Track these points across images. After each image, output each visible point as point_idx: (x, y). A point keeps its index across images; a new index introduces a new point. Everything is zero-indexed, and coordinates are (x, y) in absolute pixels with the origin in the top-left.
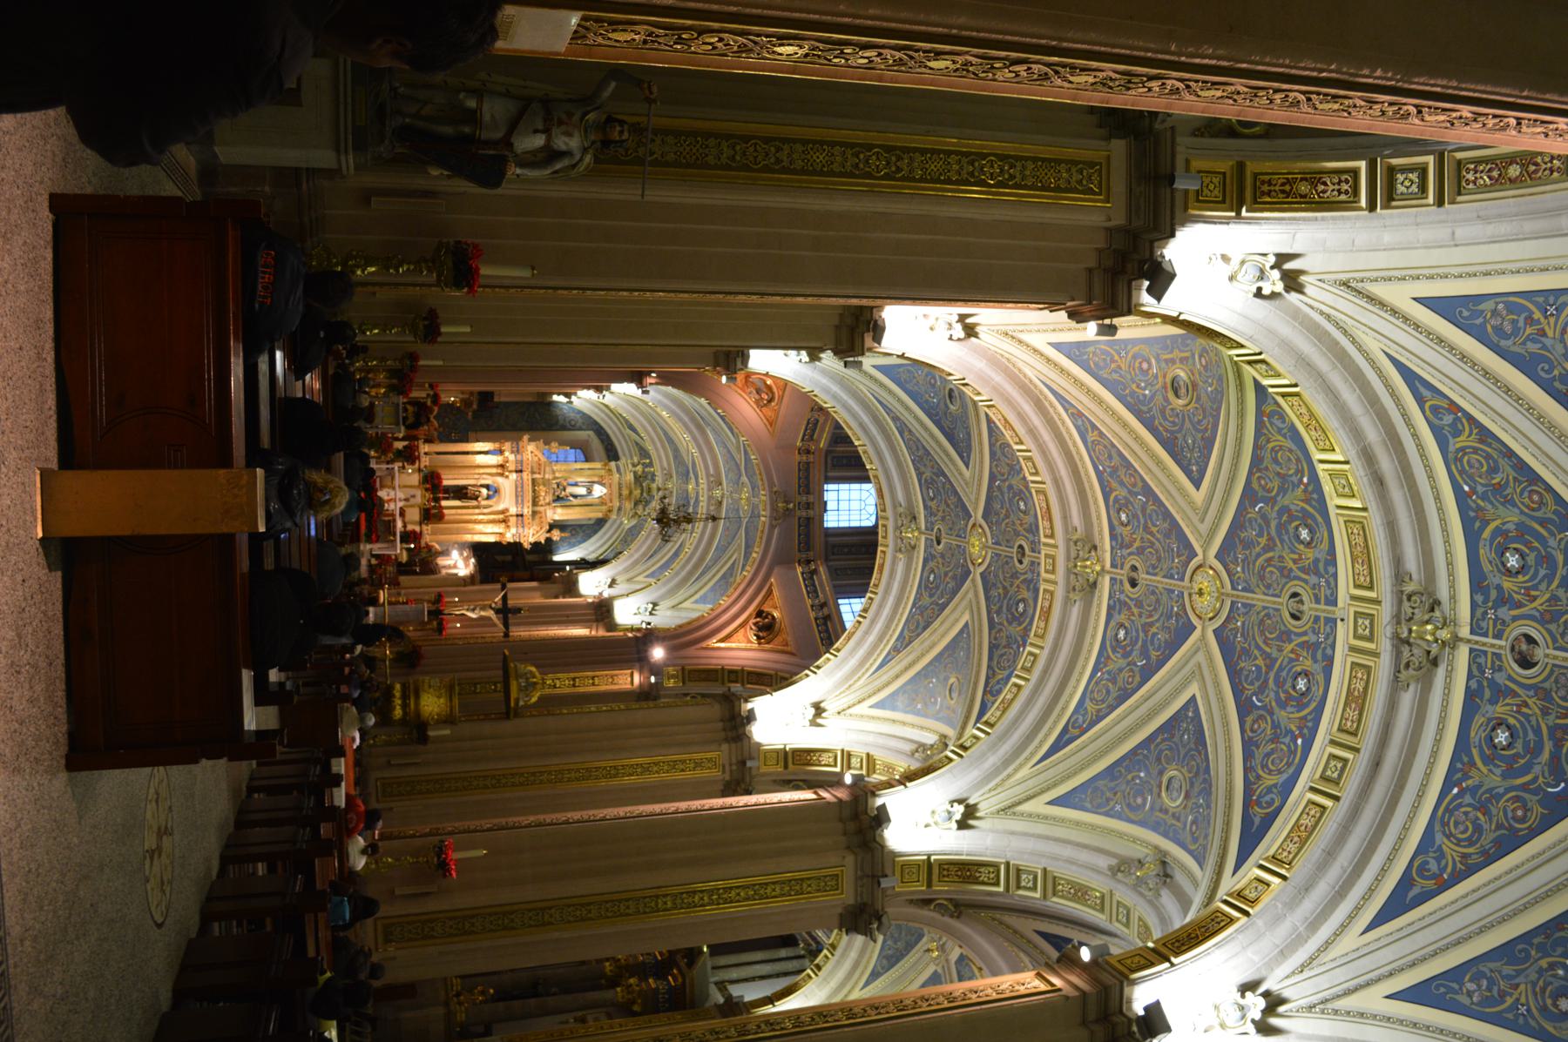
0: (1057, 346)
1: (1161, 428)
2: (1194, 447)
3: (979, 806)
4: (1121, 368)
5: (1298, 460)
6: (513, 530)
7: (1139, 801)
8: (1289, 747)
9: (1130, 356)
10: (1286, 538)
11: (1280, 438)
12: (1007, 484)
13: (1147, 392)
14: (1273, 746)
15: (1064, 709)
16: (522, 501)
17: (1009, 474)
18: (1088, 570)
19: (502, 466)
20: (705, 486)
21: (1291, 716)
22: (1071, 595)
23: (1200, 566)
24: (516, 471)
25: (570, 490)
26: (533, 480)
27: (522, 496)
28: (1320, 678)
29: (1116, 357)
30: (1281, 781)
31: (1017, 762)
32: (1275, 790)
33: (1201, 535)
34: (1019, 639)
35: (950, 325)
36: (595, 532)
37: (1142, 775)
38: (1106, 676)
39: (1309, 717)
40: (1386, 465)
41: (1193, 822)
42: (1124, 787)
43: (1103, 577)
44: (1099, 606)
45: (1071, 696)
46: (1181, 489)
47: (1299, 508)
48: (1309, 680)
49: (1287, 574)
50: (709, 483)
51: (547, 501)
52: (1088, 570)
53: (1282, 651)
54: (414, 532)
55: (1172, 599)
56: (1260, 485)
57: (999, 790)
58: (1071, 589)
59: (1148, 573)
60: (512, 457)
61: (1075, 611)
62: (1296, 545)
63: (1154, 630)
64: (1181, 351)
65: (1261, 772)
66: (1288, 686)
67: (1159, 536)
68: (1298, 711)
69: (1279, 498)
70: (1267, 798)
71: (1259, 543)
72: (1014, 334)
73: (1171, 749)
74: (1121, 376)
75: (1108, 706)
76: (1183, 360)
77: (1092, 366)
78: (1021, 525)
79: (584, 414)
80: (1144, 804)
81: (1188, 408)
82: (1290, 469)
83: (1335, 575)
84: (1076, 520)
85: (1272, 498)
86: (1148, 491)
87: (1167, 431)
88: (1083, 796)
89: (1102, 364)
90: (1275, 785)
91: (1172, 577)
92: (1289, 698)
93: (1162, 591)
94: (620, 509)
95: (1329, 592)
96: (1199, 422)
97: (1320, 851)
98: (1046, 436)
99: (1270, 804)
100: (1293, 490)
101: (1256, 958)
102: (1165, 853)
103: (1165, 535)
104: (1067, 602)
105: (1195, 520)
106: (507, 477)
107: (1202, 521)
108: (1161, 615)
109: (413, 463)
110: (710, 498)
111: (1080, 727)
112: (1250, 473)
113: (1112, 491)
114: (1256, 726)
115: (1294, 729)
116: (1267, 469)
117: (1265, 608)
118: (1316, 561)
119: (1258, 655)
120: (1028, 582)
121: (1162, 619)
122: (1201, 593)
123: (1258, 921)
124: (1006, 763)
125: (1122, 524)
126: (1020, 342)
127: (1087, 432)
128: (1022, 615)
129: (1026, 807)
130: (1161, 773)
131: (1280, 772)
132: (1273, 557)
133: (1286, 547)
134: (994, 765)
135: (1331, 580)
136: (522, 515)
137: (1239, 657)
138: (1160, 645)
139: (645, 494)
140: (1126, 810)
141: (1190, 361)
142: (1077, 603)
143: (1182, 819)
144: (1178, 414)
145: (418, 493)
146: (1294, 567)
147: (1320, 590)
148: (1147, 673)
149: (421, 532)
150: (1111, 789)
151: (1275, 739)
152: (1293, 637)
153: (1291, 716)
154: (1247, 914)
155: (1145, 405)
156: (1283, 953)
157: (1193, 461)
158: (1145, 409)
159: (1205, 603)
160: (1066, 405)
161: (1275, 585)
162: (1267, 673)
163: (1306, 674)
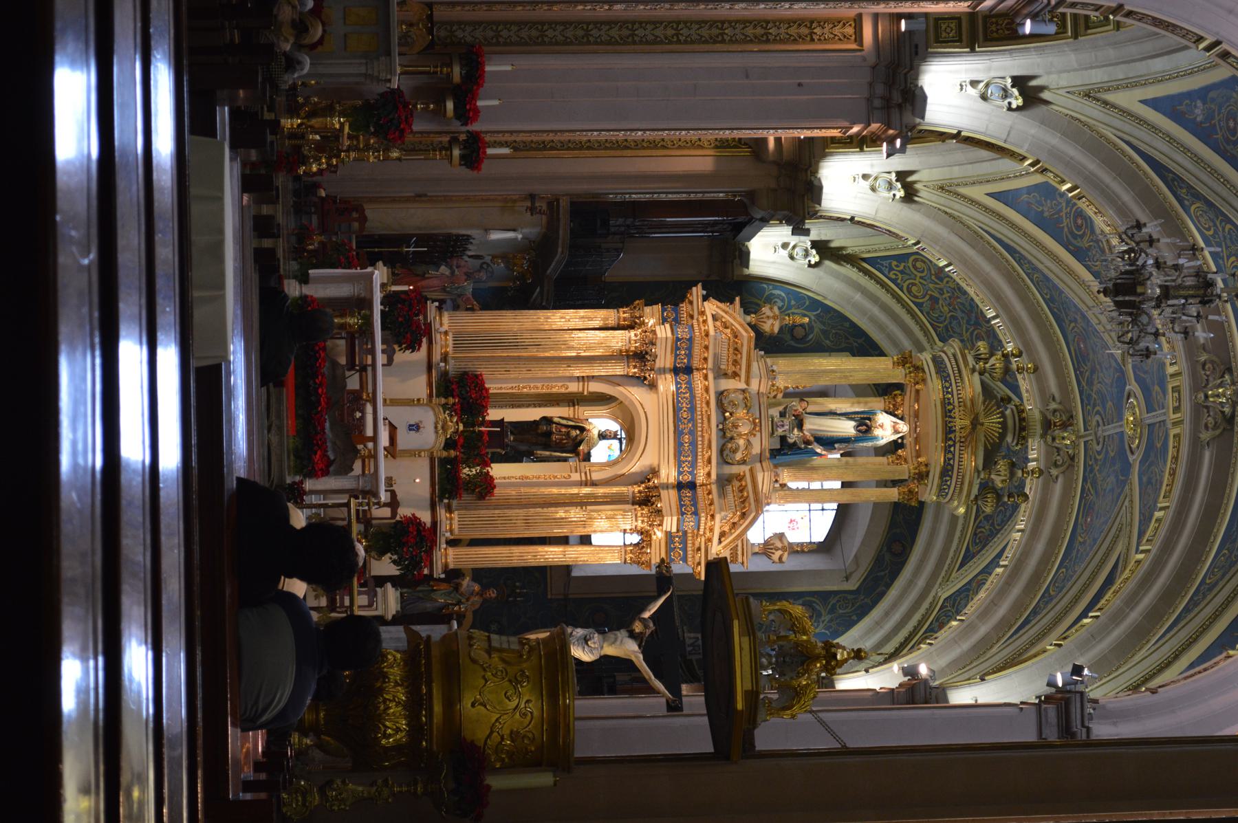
6: (670, 523)
16: (693, 444)
19: (640, 357)
20: (1184, 382)
24: (676, 371)
25: (813, 425)
26: (720, 395)
27: (692, 433)
36: (863, 612)
50: (1195, 367)
51: (756, 450)
54: (414, 521)
60: (664, 332)
79: (828, 309)
94: (946, 472)
106: (653, 386)
109: (413, 346)
110: (1199, 409)
136: (692, 486)
139: (1009, 439)
145: (427, 417)
149: (434, 523)
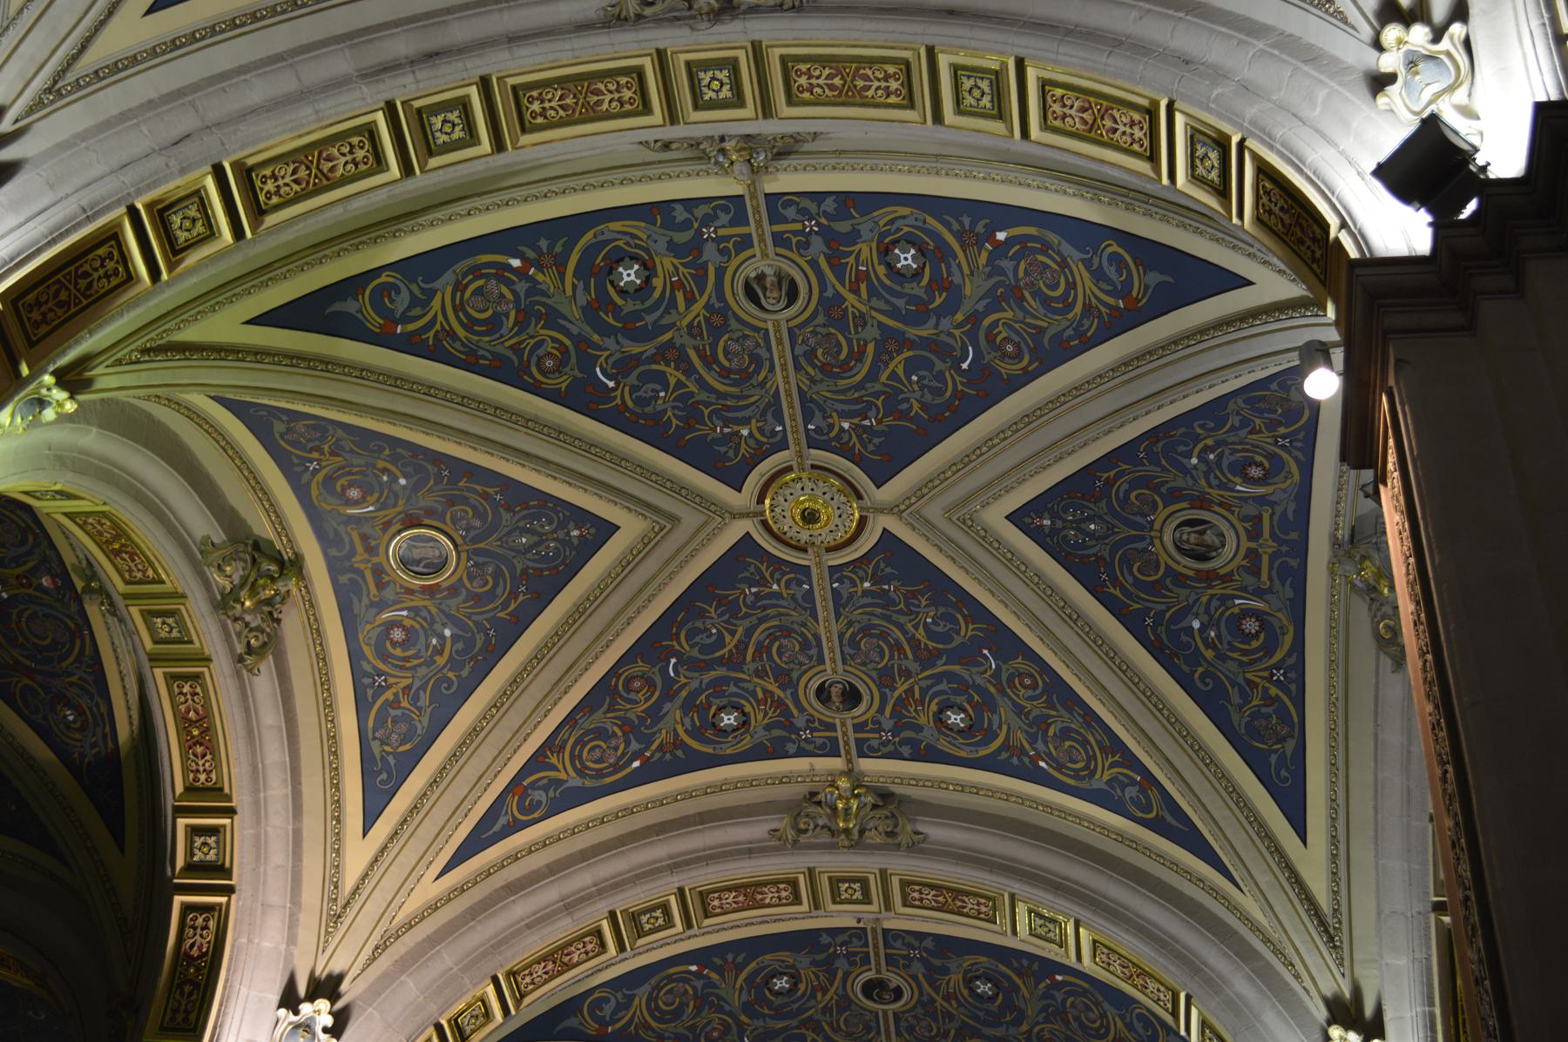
0: (370, 819)
1: (512, 607)
2: (531, 532)
3: (1328, 993)
4: (409, 687)
5: (476, 271)
7: (1251, 626)
8: (1018, 258)
9: (381, 666)
10: (650, 319)
11: (436, 304)
12: (743, 1018)
13: (447, 633)
14: (1027, 294)
15: (1121, 837)
17: (720, 1009)
18: (854, 804)
21: (966, 271)
22: (903, 839)
23: (764, 523)
28: (883, 215)
29: (389, 695)
30: (1077, 255)
31: (1243, 931)
32: (1096, 261)
33: (705, 524)
34: (1042, 985)
35: (297, 1026)
37: (1196, 625)
38: (1040, 746)
39: (956, 226)
40: (400, 46)
41: (1249, 480)
42: (1230, 664)
43: (863, 774)
44: (917, 781)
45: (1104, 828)
46: (627, 564)
47: (581, 286)
48: (895, 242)
49: (719, 319)
52: (854, 804)
53: (862, 315)
55: (852, 595)
56: (557, 370)
57: (1290, 951)
58: (892, 839)
59: (821, 661)
61: (937, 832)
62: (657, 294)
63: (921, 634)
64: (353, 552)
65: (1078, 308)
66: (918, 289)
67: (740, 630)
68: (955, 257)
69: (575, 331)
70: (1111, 272)
71: (679, 384)
72: (341, 902)
73: (1126, 562)
74: (423, 687)
75: (1089, 727)
76: (371, 550)
77: (408, 747)
78: (825, 991)
80: (1257, 615)
81: (459, 541)
82: (502, 296)
83: (689, 203)
84: (755, 831)
85: (576, 347)
86: (650, 647)
87: (514, 594)
88: (1273, 758)
89: (403, 727)
90: (1087, 264)
91: (809, 596)
92: (937, 284)
93: (843, 621)
95: (724, 218)
96: (479, 514)
97: (1111, 60)
98: (582, 879)
99: (1114, 258)
100: (545, 294)
101: (1321, 94)
102: (1335, 543)
103: (734, 615)
104: (918, 846)
105: (679, 536)
107: (674, 519)
108: (888, 619)
111: (1143, 791)
112: (536, 390)
113: (678, 743)
114: (1010, 348)
115: (984, 255)
116: (516, 349)
117: (798, 367)
118: (673, 248)
119: (888, 372)
120: (934, 974)
121: (895, 617)
122: (810, 517)
123: (1248, 117)
124: (1245, 954)
125: (745, 724)
126: (356, 891)
127: (560, 782)
128: (996, 984)
129: (1320, 889)
130: (1179, 579)
131: (1063, 264)
132: (696, 348)
133: (667, 320)
134: (1249, 978)
135: (700, 211)
137: (904, 415)
138: (944, 617)
140: (1278, 656)
141: (367, 529)
142: (920, 828)
143: (1250, 510)
144: (476, 565)
146: (702, 301)
147: (727, 238)
148: (1008, 643)
150: (1246, 699)
151: (1014, 294)
152: (829, 293)
153: (966, 271)
154: (1241, 145)
155: (473, 641)
156: (1311, 56)
157: (561, 534)
158: (480, 639)
159: (836, 518)
160: (502, 821)
161: (749, 343)
162: (911, 344)
163: (885, 251)
